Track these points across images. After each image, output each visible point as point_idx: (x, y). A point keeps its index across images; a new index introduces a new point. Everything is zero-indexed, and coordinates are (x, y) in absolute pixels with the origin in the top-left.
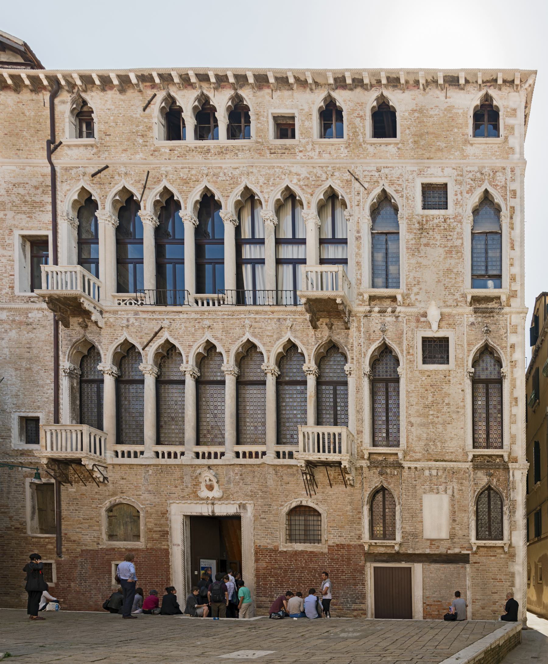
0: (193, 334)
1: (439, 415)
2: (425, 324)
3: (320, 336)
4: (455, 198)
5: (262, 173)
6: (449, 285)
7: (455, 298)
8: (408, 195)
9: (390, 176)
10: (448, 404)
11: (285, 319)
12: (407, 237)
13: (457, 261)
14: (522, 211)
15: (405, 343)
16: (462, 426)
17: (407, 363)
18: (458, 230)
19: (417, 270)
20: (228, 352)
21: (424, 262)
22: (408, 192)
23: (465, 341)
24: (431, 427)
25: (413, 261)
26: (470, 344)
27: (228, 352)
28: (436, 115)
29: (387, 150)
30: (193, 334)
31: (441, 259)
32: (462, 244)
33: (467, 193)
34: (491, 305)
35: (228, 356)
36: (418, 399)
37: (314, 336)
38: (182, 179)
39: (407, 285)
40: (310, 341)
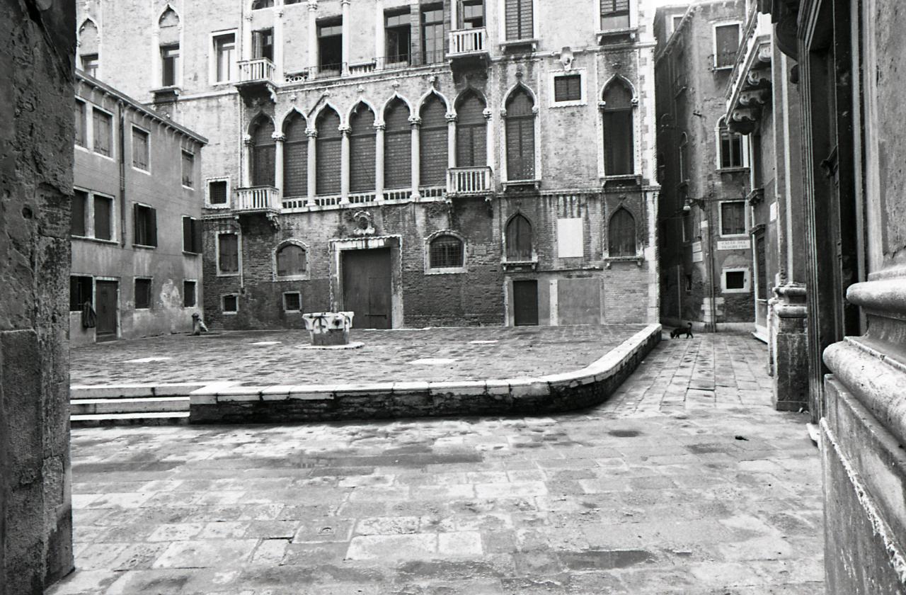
35: (379, 114)
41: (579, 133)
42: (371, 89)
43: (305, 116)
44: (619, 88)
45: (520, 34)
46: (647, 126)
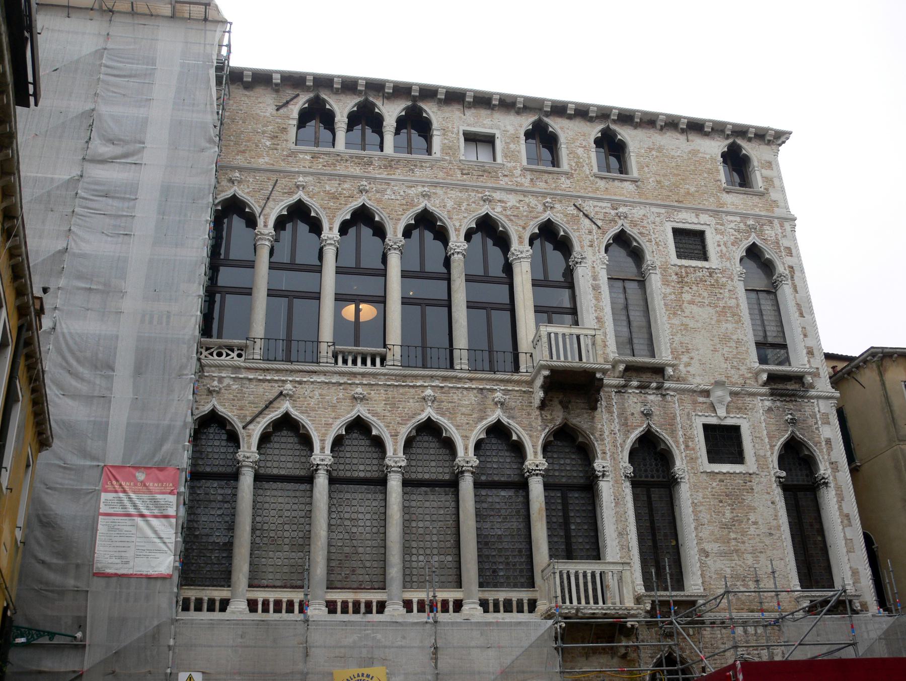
0: (334, 407)
2: (704, 406)
3: (549, 417)
4: (718, 249)
7: (741, 373)
10: (755, 523)
11: (492, 391)
12: (663, 291)
15: (680, 433)
16: (781, 556)
17: (687, 462)
18: (729, 287)
21: (692, 324)
23: (765, 432)
24: (736, 557)
25: (676, 321)
27: (395, 435)
30: (334, 407)
31: (713, 322)
32: (738, 305)
33: (733, 244)
34: (791, 386)
35: (395, 443)
37: (540, 418)
38: (328, 193)
39: (672, 353)
40: (534, 424)
41: (752, 518)
42: (378, 397)
43: (239, 426)
44: (796, 456)
45: (288, 350)
46: (847, 516)
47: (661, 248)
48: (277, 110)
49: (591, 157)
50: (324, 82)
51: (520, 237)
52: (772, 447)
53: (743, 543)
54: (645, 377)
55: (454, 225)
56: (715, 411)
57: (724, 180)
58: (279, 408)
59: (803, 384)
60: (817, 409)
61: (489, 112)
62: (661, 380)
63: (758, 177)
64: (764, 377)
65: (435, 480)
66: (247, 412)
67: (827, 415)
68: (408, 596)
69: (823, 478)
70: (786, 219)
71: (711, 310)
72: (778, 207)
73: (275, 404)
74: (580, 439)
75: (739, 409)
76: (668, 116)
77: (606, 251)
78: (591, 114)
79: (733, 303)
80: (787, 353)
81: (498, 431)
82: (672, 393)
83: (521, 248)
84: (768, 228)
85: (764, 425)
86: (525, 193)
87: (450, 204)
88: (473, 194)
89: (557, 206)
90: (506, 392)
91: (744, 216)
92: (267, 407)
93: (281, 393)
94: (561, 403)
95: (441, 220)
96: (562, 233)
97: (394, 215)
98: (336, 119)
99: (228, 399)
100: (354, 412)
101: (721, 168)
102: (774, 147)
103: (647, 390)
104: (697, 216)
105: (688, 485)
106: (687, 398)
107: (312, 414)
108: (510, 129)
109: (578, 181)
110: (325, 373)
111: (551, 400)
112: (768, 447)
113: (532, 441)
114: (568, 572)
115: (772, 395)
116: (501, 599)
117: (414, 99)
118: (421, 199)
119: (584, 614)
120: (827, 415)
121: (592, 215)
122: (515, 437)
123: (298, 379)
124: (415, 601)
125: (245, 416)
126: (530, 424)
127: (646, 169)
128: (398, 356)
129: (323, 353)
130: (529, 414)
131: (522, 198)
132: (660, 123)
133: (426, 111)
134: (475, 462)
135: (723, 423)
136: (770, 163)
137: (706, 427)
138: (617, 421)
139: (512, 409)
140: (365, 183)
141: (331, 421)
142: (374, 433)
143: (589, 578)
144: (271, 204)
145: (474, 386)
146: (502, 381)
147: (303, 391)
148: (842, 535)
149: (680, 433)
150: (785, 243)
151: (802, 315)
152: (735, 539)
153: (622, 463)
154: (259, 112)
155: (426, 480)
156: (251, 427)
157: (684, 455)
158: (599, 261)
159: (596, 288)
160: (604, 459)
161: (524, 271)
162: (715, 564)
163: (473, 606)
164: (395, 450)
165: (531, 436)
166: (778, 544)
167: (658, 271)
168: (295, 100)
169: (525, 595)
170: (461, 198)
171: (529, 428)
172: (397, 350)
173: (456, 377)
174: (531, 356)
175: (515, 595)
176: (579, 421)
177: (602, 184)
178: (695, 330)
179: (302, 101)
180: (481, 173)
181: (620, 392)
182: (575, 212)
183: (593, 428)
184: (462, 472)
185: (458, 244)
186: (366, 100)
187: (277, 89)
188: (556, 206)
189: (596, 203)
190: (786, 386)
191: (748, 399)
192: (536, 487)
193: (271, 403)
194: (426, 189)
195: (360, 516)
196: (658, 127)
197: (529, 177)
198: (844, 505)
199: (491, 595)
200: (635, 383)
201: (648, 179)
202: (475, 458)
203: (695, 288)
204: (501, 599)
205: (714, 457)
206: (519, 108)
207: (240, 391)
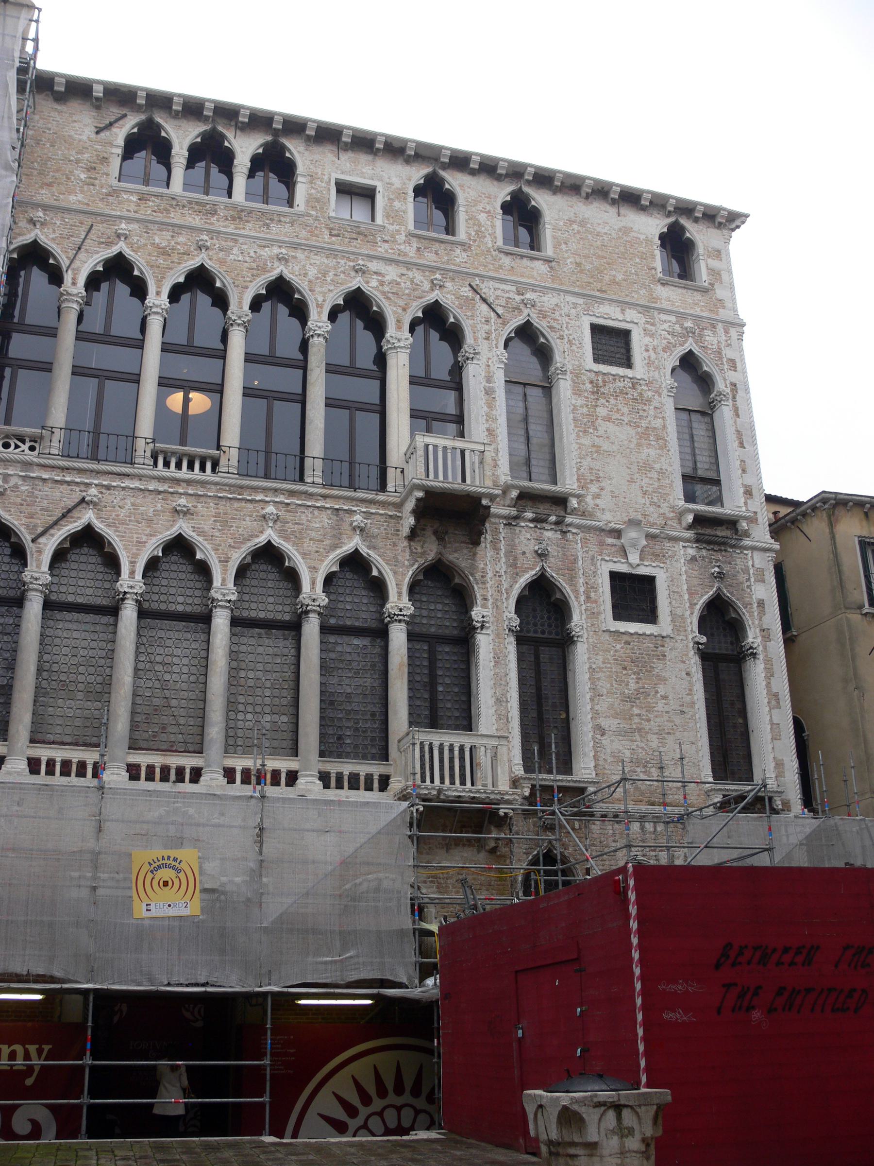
1: (651, 716)
2: (613, 549)
3: (420, 550)
4: (646, 354)
5: (312, 261)
6: (650, 489)
7: (662, 511)
8: (571, 338)
9: (539, 304)
10: (665, 697)
11: (351, 512)
12: (574, 402)
13: (658, 451)
14: (747, 390)
15: (581, 581)
16: (693, 739)
17: (587, 618)
18: (655, 403)
19: (594, 456)
20: (225, 561)
21: (605, 446)
22: (570, 332)
23: (685, 587)
24: (638, 738)
25: (586, 441)
26: (693, 594)
27: (225, 561)
28: (606, 234)
29: (533, 266)
30: (149, 520)
31: (632, 446)
32: (664, 427)
33: (664, 350)
34: (721, 532)
35: (225, 571)
36: (612, 686)
37: (408, 550)
38: (158, 247)
39: (578, 479)
40: (400, 558)
42: (206, 510)
43: (27, 538)
44: (721, 619)
45: (95, 446)
46: (776, 695)
47: (574, 347)
48: (97, 133)
49: (496, 226)
50: (160, 101)
51: (398, 321)
52: (692, 605)
53: (649, 720)
54: (543, 509)
55: (316, 300)
56: (626, 556)
57: (660, 269)
58: (79, 518)
59: (737, 530)
60: (750, 563)
61: (370, 157)
62: (562, 513)
63: (702, 269)
64: (690, 518)
65: (272, 621)
66: (39, 521)
67: (763, 570)
68: (230, 763)
69: (751, 648)
70: (733, 324)
71: (632, 431)
72: (724, 307)
73: (75, 513)
74: (457, 580)
75: (656, 556)
76: (597, 181)
77: (506, 346)
78: (499, 171)
79: (658, 423)
80: (720, 491)
81: (355, 563)
82: (574, 531)
83: (399, 335)
84: (710, 333)
85: (684, 577)
86: (409, 265)
87: (312, 272)
88: (342, 262)
89: (449, 285)
90: (368, 515)
91: (682, 316)
92: (64, 516)
93: (83, 500)
94: (435, 533)
95: (300, 292)
96: (452, 320)
97: (240, 281)
98: (173, 152)
99: (15, 503)
100: (174, 529)
101: (657, 253)
102: (725, 232)
103: (544, 525)
104: (623, 311)
105: (586, 646)
106: (592, 537)
107: (122, 528)
108: (395, 181)
109: (477, 254)
110: (140, 477)
111: (424, 529)
112: (688, 605)
113: (396, 579)
114: (431, 744)
115: (697, 541)
116: (346, 773)
117: (276, 133)
118: (276, 264)
119: (448, 796)
120: (763, 570)
121: (491, 300)
122: (375, 573)
123: (105, 483)
124: (239, 769)
125: (35, 526)
126: (395, 557)
127: (563, 247)
128: (234, 462)
129: (140, 452)
130: (395, 545)
131: (404, 271)
132: (586, 190)
133: (289, 150)
134: (323, 600)
135: (634, 572)
136: (719, 251)
137: (614, 576)
138: (503, 560)
139: (373, 537)
140: (205, 237)
141: (144, 538)
142: (198, 557)
143: (456, 753)
144: (82, 255)
145: (327, 506)
146: (363, 501)
147: (111, 498)
148: (768, 718)
149: (581, 581)
150: (728, 353)
151: (742, 445)
152: (639, 715)
153: (506, 614)
154: (72, 133)
155: (261, 620)
156: (42, 540)
157: (583, 607)
158: (495, 358)
159: (489, 392)
160: (484, 606)
161: (401, 364)
162: (612, 744)
163: (310, 779)
164: (224, 580)
165: (395, 573)
166: (690, 725)
167: (568, 376)
168: (121, 122)
169: (376, 769)
170: (327, 266)
171: (394, 562)
172: (234, 454)
173: (306, 493)
174: (402, 472)
175: (363, 769)
176: (457, 557)
177: (506, 261)
178: (609, 454)
179: (130, 123)
180: (354, 236)
181: (509, 524)
182: (470, 294)
183: (473, 567)
184: (307, 612)
185: (320, 324)
186: (214, 129)
187: (98, 105)
188: (447, 284)
189: (497, 285)
190: (715, 532)
191: (668, 544)
192: (398, 636)
193: (69, 511)
194: (283, 251)
195: (176, 660)
196: (584, 194)
197: (415, 245)
198: (773, 681)
199: (334, 767)
200: (529, 515)
201: (565, 259)
202: (323, 596)
203: (612, 401)
204: (346, 773)
205: (621, 612)
206: (409, 156)
207: (31, 494)
